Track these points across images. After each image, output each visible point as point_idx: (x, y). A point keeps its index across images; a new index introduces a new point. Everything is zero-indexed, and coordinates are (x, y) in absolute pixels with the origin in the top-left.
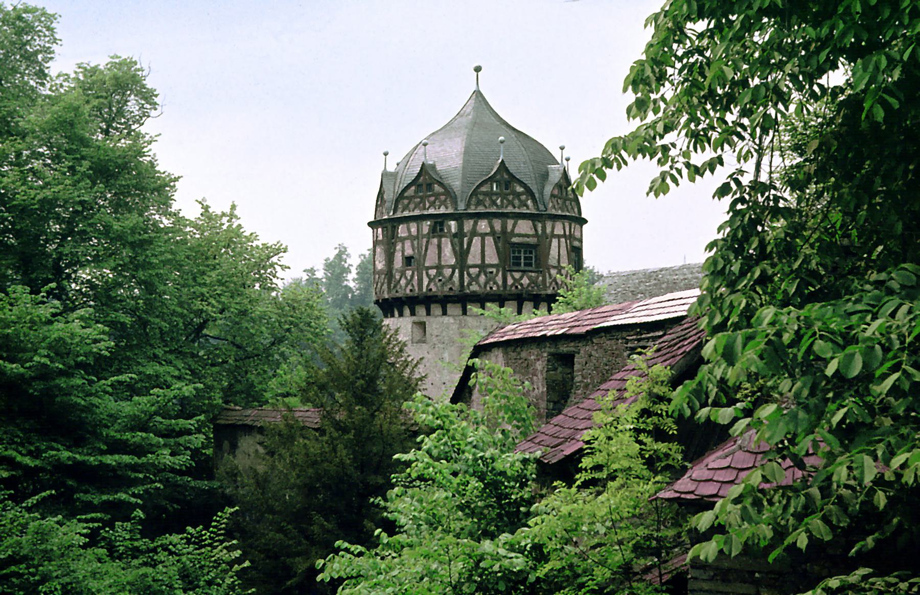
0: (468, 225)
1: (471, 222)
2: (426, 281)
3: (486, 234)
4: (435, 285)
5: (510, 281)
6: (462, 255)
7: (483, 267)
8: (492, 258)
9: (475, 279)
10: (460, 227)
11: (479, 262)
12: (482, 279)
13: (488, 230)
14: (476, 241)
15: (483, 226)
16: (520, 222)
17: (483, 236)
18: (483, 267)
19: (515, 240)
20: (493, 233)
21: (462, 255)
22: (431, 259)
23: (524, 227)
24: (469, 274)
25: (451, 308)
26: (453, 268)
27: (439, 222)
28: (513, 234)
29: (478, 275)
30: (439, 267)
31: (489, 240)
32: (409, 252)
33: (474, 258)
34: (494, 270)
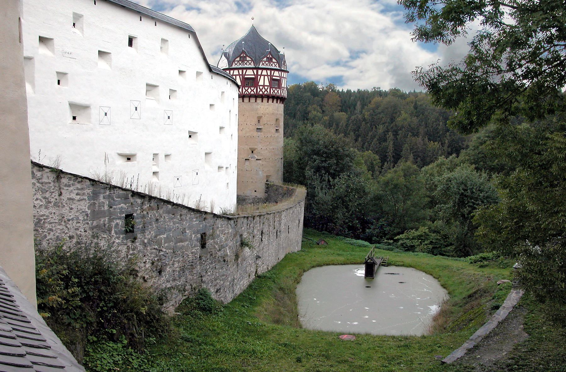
0: (260, 72)
5: (272, 91)
7: (264, 86)
8: (267, 83)
9: (261, 90)
10: (257, 72)
12: (264, 90)
14: (262, 77)
15: (264, 72)
17: (264, 76)
18: (264, 86)
20: (267, 75)
23: (276, 73)
25: (253, 100)
28: (273, 76)
31: (266, 77)
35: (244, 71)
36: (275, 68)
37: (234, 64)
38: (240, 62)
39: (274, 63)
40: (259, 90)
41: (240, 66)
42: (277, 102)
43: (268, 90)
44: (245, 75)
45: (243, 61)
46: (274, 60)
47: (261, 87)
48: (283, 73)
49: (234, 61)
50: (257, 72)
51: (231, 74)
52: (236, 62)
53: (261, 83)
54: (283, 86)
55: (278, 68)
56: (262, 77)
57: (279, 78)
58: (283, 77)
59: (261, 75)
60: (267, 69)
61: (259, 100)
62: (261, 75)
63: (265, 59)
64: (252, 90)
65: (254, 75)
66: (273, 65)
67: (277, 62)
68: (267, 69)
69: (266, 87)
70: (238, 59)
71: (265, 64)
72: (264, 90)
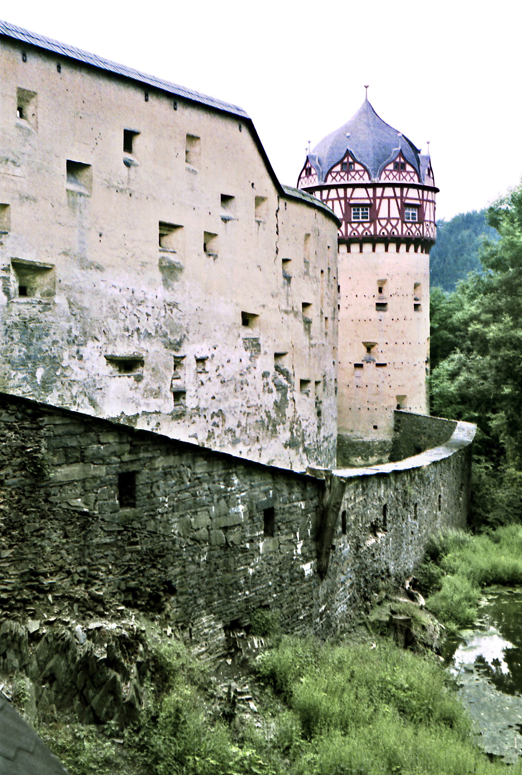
3: (392, 198)
5: (405, 229)
8: (395, 213)
9: (385, 227)
11: (387, 216)
12: (389, 228)
13: (393, 195)
14: (385, 202)
15: (389, 192)
16: (411, 190)
17: (389, 198)
18: (389, 219)
23: (413, 193)
31: (393, 202)
35: (349, 190)
36: (412, 182)
37: (330, 178)
38: (342, 174)
39: (408, 173)
41: (343, 182)
42: (416, 251)
43: (399, 227)
44: (351, 198)
45: (348, 172)
46: (409, 168)
48: (426, 192)
49: (330, 172)
51: (325, 197)
52: (334, 175)
53: (383, 213)
54: (427, 218)
55: (416, 182)
57: (418, 202)
58: (427, 201)
59: (382, 198)
60: (393, 186)
61: (380, 247)
63: (391, 167)
65: (369, 198)
66: (408, 178)
68: (393, 186)
69: (394, 222)
70: (338, 168)
71: (391, 176)
72: (389, 228)
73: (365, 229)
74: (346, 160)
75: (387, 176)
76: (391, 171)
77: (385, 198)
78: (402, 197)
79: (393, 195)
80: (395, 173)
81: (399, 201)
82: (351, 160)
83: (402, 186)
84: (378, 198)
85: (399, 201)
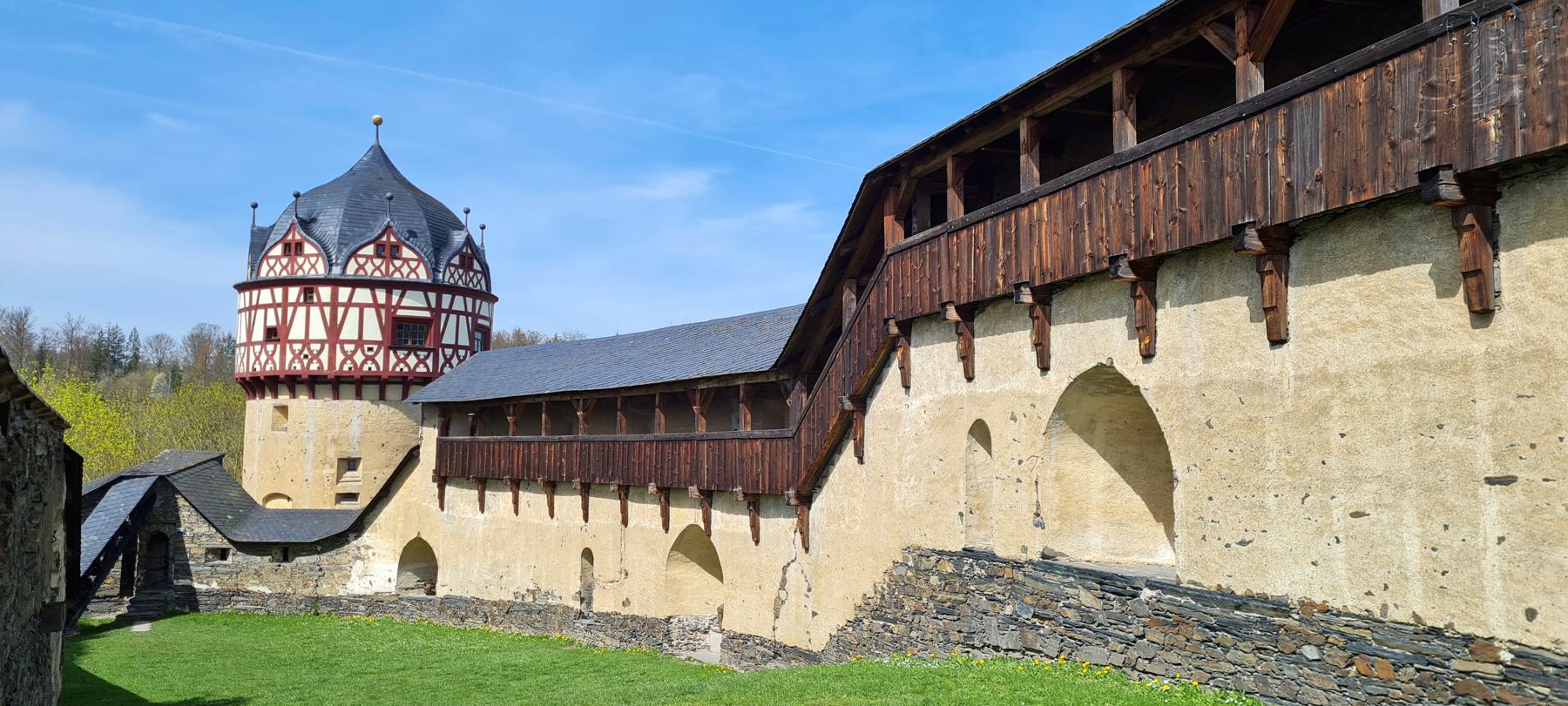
0: (344, 293)
1: (349, 290)
2: (289, 356)
3: (369, 305)
4: (301, 362)
6: (334, 329)
8: (373, 332)
11: (356, 337)
12: (359, 358)
13: (370, 301)
14: (354, 313)
15: (363, 295)
17: (362, 307)
18: (360, 343)
19: (400, 313)
20: (376, 305)
21: (334, 329)
22: (297, 332)
24: (344, 352)
26: (322, 342)
27: (309, 286)
29: (354, 352)
30: (306, 342)
31: (370, 314)
32: (272, 322)
33: (349, 331)
34: (375, 347)
40: (340, 357)
43: (380, 359)
45: (292, 261)
47: (349, 348)
50: (335, 295)
52: (272, 262)
56: (354, 313)
57: (427, 314)
59: (348, 305)
60: (372, 284)
61: (371, 391)
62: (348, 305)
64: (421, 361)
66: (405, 270)
67: (420, 260)
68: (372, 284)
72: (359, 358)
73: (403, 361)
74: (290, 237)
75: (361, 267)
76: (368, 257)
77: (356, 305)
78: (388, 306)
79: (370, 301)
80: (378, 262)
81: (383, 312)
82: (298, 237)
83: (389, 286)
84: (343, 305)
85: (383, 312)
